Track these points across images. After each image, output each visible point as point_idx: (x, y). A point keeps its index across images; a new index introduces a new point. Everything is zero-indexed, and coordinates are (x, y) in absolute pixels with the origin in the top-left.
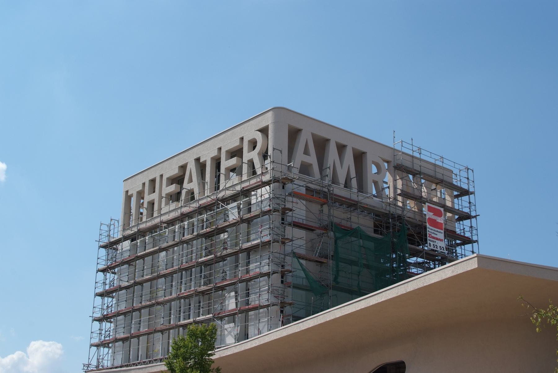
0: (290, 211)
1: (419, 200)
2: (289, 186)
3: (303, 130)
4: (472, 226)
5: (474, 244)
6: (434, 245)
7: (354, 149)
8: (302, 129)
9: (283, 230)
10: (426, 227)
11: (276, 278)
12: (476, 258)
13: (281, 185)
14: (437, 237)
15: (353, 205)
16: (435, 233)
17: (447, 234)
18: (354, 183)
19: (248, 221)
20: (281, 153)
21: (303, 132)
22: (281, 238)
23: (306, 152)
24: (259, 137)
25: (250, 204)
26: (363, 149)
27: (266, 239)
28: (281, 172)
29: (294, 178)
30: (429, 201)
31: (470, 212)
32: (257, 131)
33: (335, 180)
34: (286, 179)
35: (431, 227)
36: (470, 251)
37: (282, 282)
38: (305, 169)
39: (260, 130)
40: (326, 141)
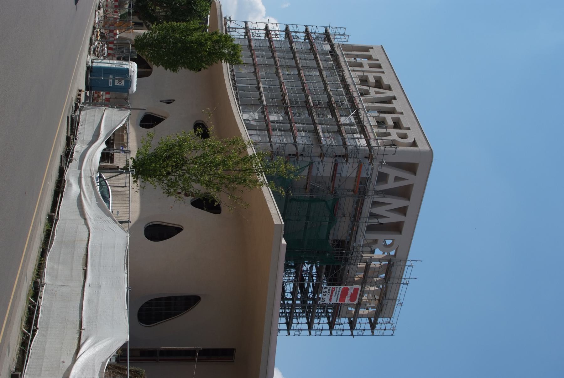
0: (346, 161)
1: (364, 282)
2: (367, 161)
3: (415, 176)
4: (345, 331)
5: (329, 331)
6: (326, 292)
7: (403, 222)
8: (416, 176)
9: (331, 155)
10: (341, 286)
11: (293, 150)
12: (281, 224)
13: (368, 156)
14: (333, 296)
15: (356, 218)
16: (337, 295)
17: (336, 305)
18: (374, 221)
19: (339, 132)
20: (393, 155)
21: (414, 176)
22: (323, 153)
23: (397, 179)
24: (410, 140)
25: (353, 133)
26: (404, 231)
27: (324, 142)
28: (378, 154)
29: (373, 165)
30: (362, 290)
31: (357, 330)
32: (414, 139)
33: (375, 204)
34: (372, 159)
35: (341, 291)
36: (322, 328)
37: (290, 155)
38: (383, 178)
39: (414, 141)
40: (408, 198)
